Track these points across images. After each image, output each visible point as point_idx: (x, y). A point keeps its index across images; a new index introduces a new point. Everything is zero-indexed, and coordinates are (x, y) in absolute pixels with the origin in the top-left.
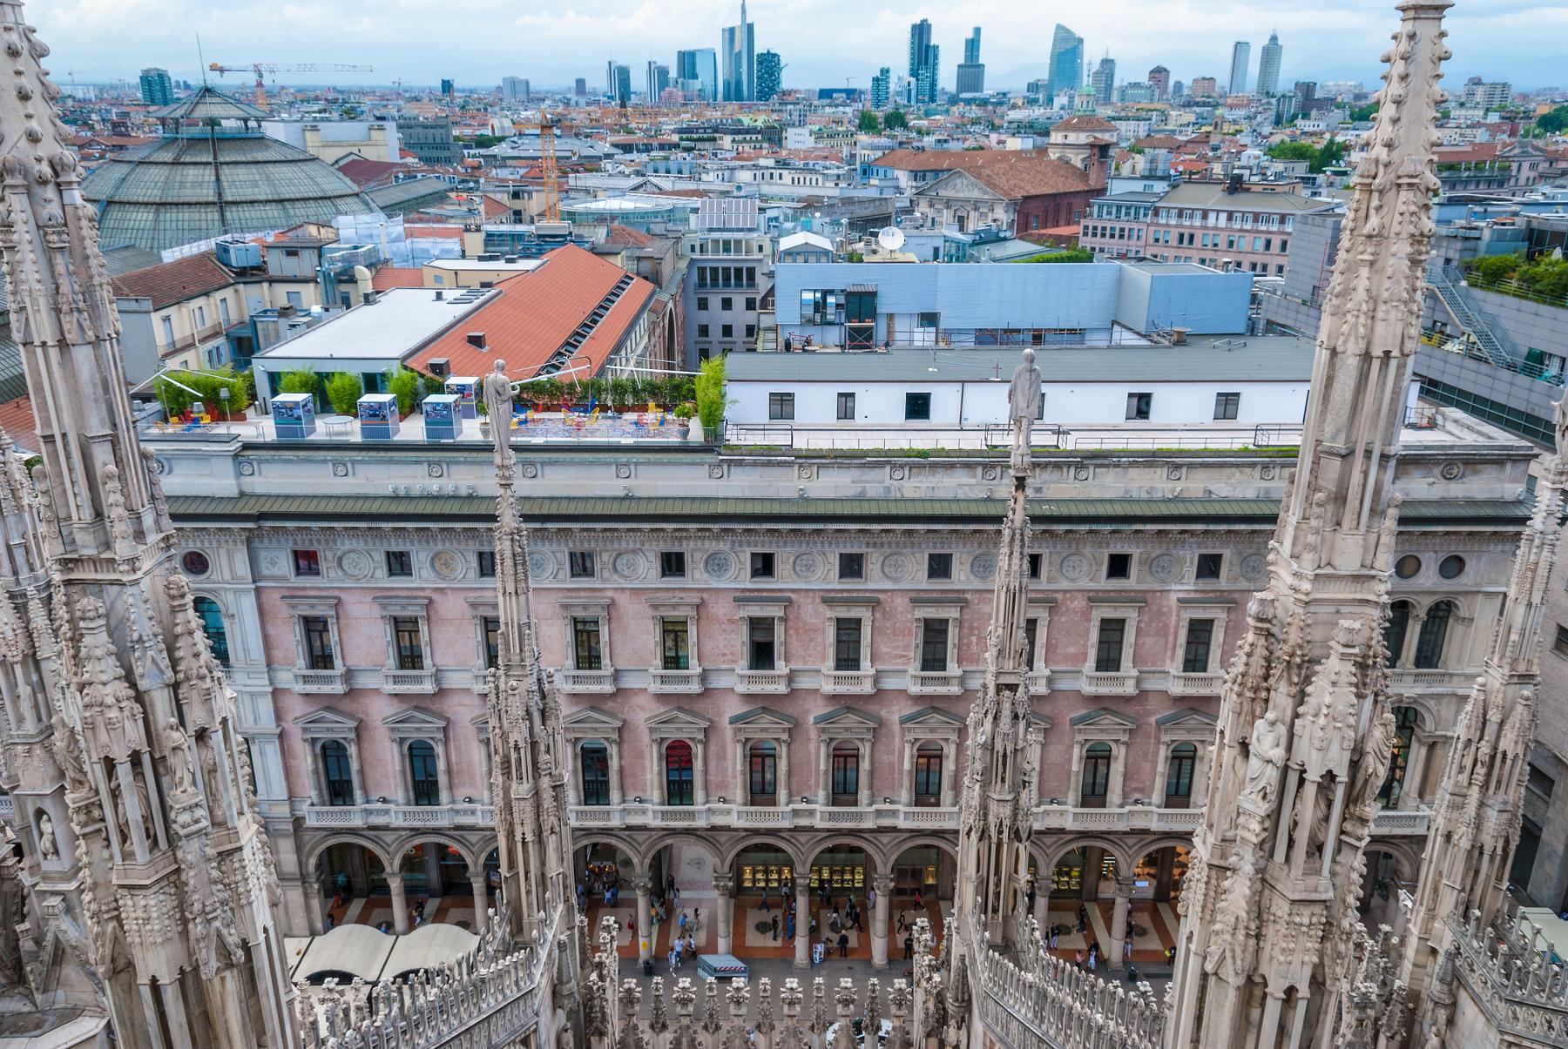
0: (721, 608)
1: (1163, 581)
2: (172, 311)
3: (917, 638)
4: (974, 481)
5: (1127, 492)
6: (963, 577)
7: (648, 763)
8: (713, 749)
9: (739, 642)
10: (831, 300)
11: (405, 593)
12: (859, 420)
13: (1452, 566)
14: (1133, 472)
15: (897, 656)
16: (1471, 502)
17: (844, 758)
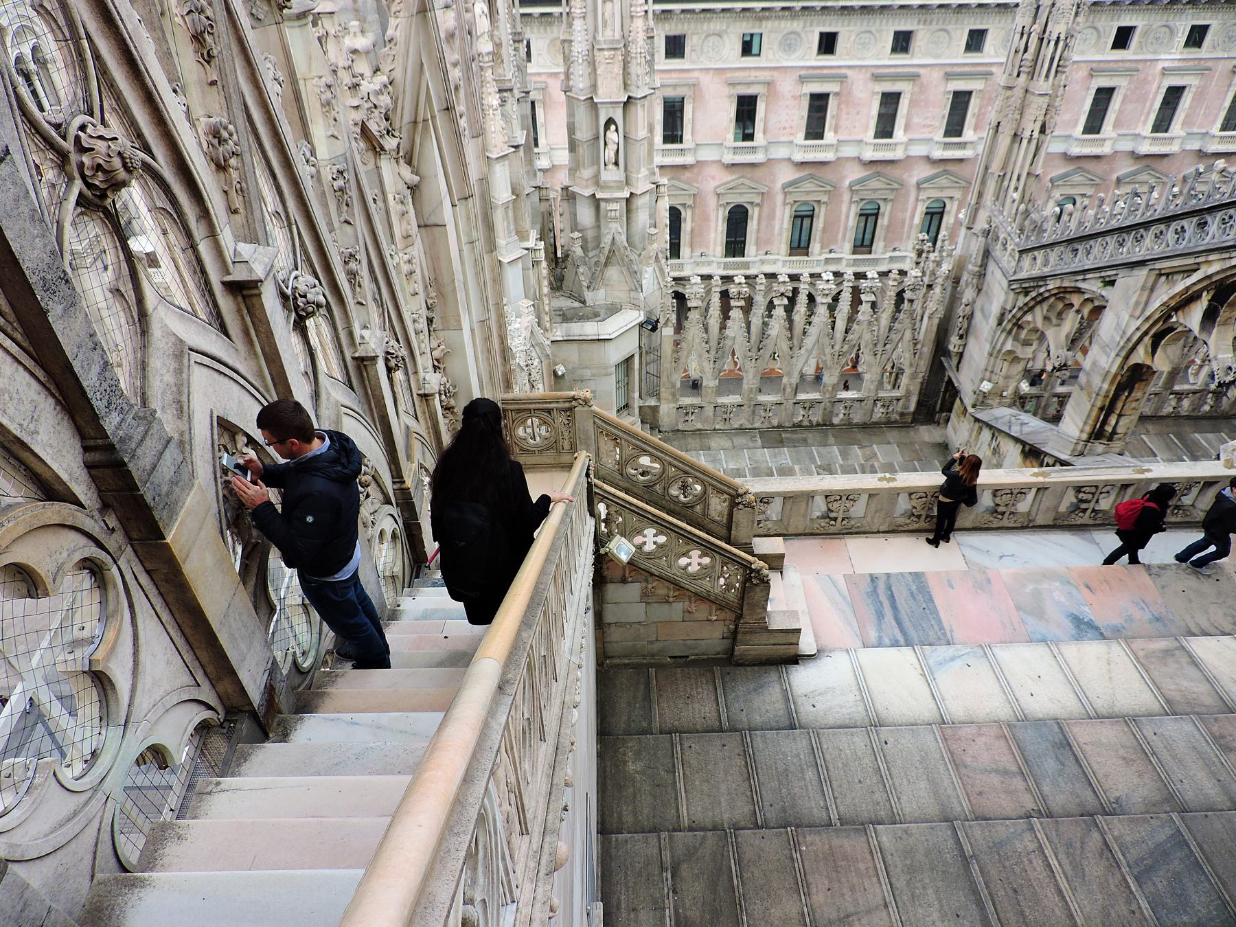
0: (787, 86)
1: (1155, 53)
3: (942, 110)
6: (992, 52)
7: (713, 225)
8: (766, 210)
9: (799, 114)
15: (925, 126)
17: (870, 217)
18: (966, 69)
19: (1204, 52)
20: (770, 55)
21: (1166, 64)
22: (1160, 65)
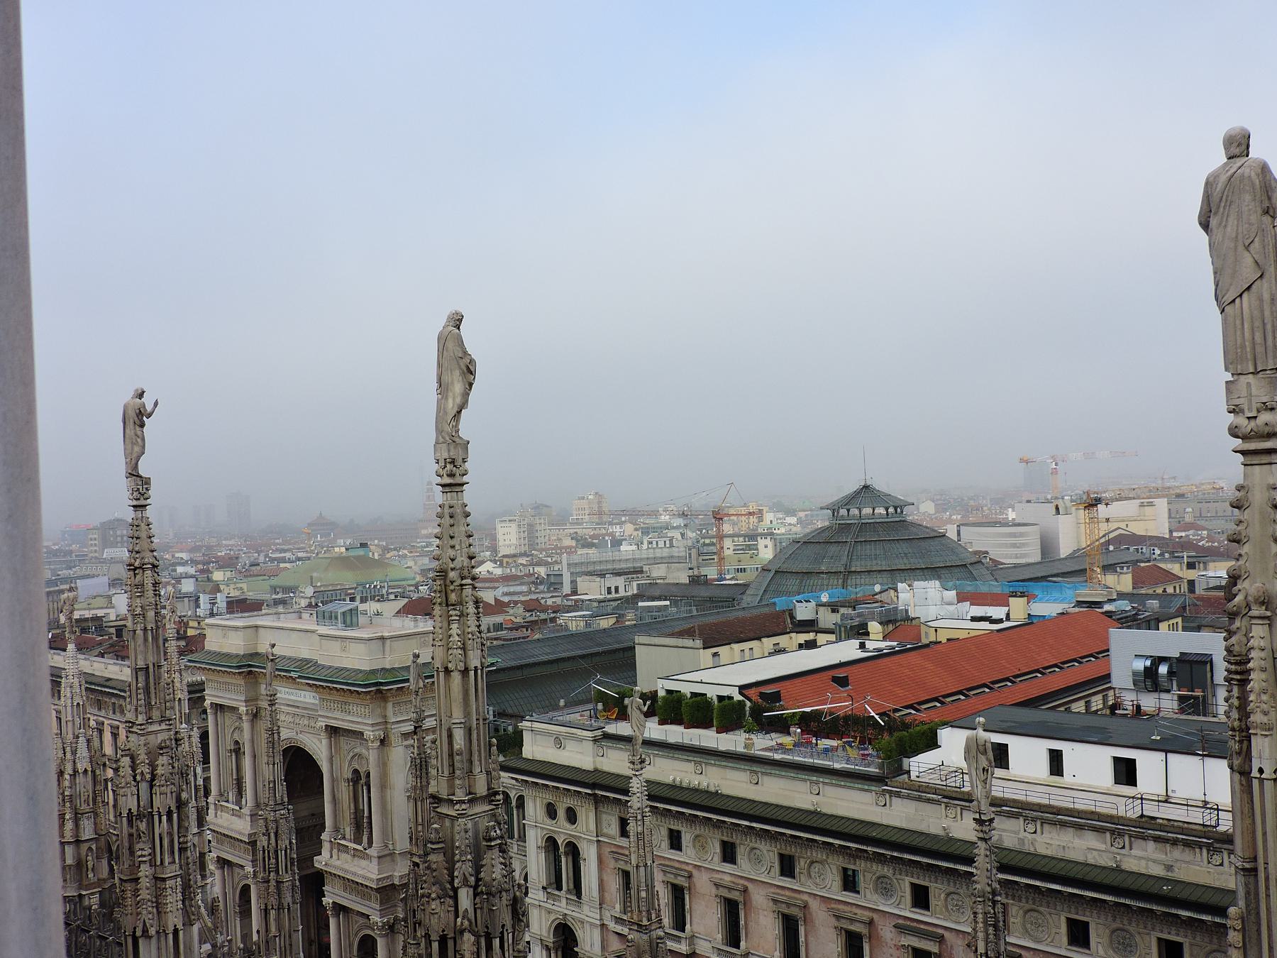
2: (723, 650)
4: (1103, 847)
10: (1163, 669)
11: (677, 865)
12: (1067, 779)
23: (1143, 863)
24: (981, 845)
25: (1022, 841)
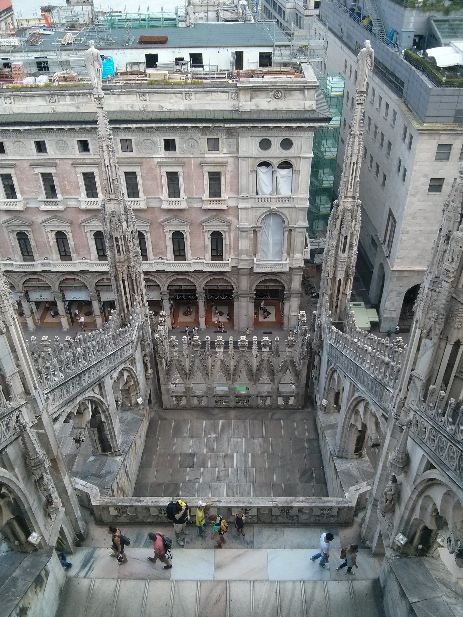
4: (45, 103)
5: (121, 107)
6: (53, 153)
13: (287, 144)
14: (123, 97)
15: (32, 192)
16: (290, 111)
18: (38, 162)
19: (178, 153)
20: (52, 151)
21: (159, 160)
22: (156, 161)
23: (66, 107)
24: (100, 111)
25: (5, 109)
